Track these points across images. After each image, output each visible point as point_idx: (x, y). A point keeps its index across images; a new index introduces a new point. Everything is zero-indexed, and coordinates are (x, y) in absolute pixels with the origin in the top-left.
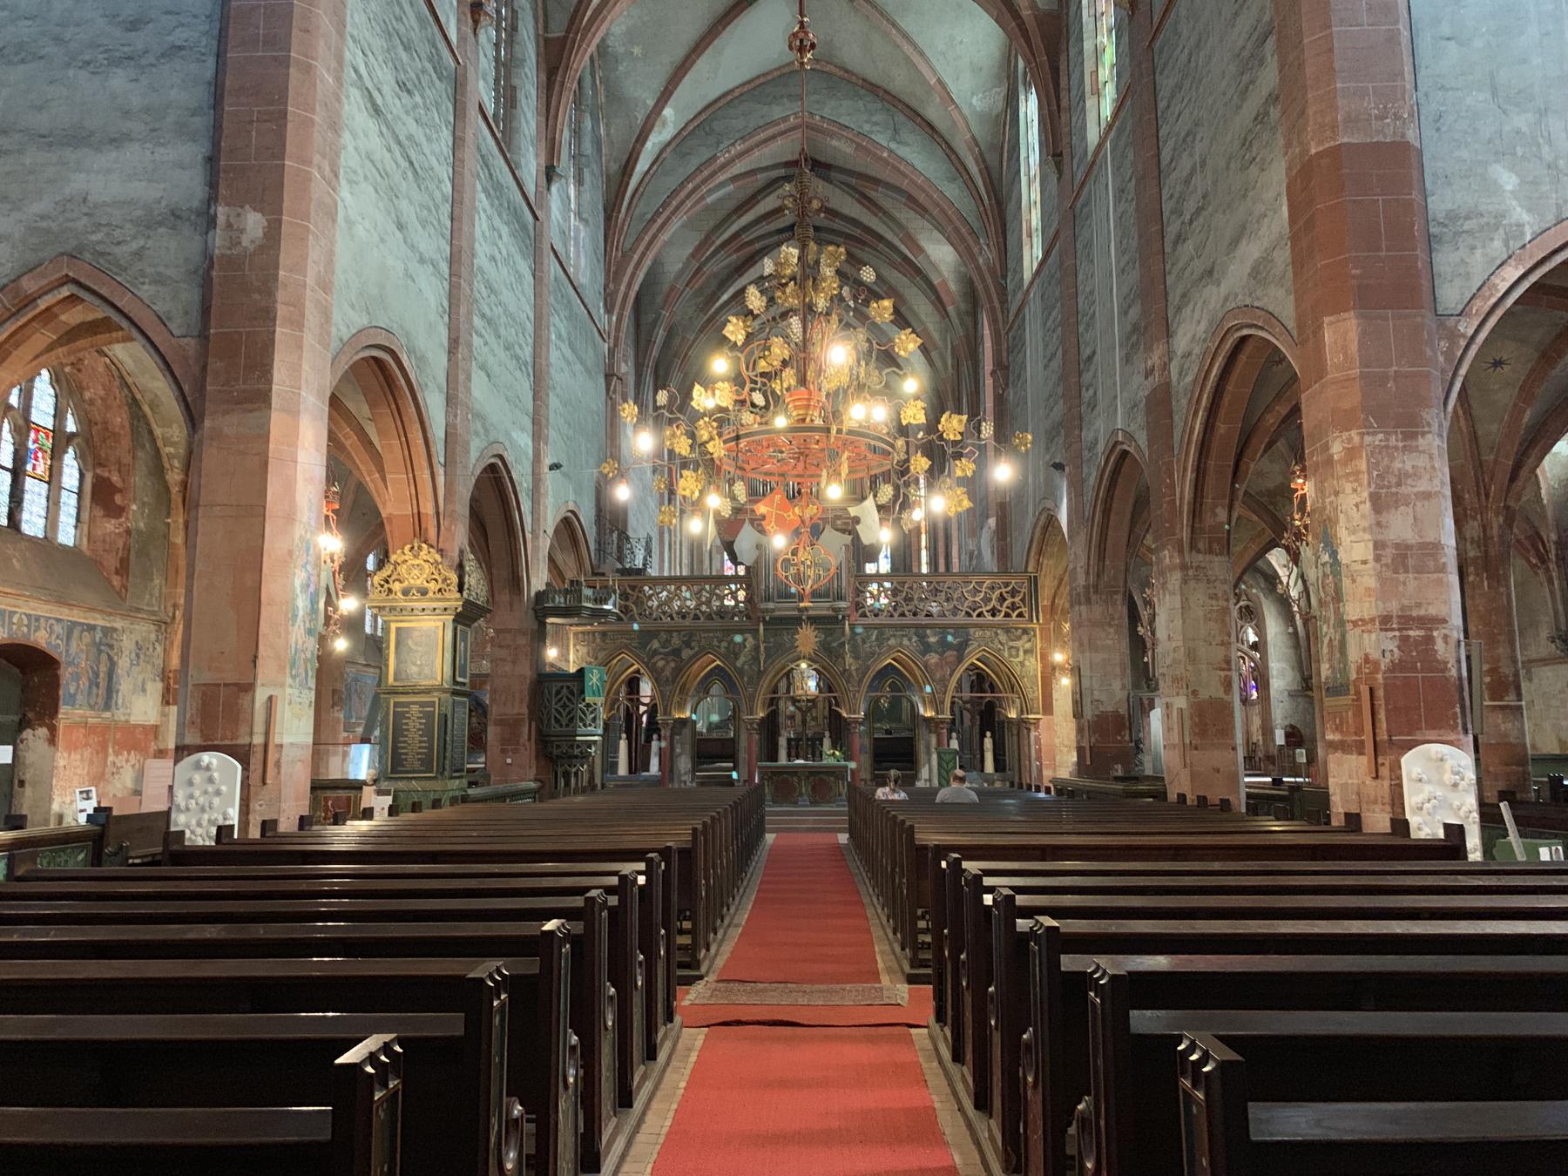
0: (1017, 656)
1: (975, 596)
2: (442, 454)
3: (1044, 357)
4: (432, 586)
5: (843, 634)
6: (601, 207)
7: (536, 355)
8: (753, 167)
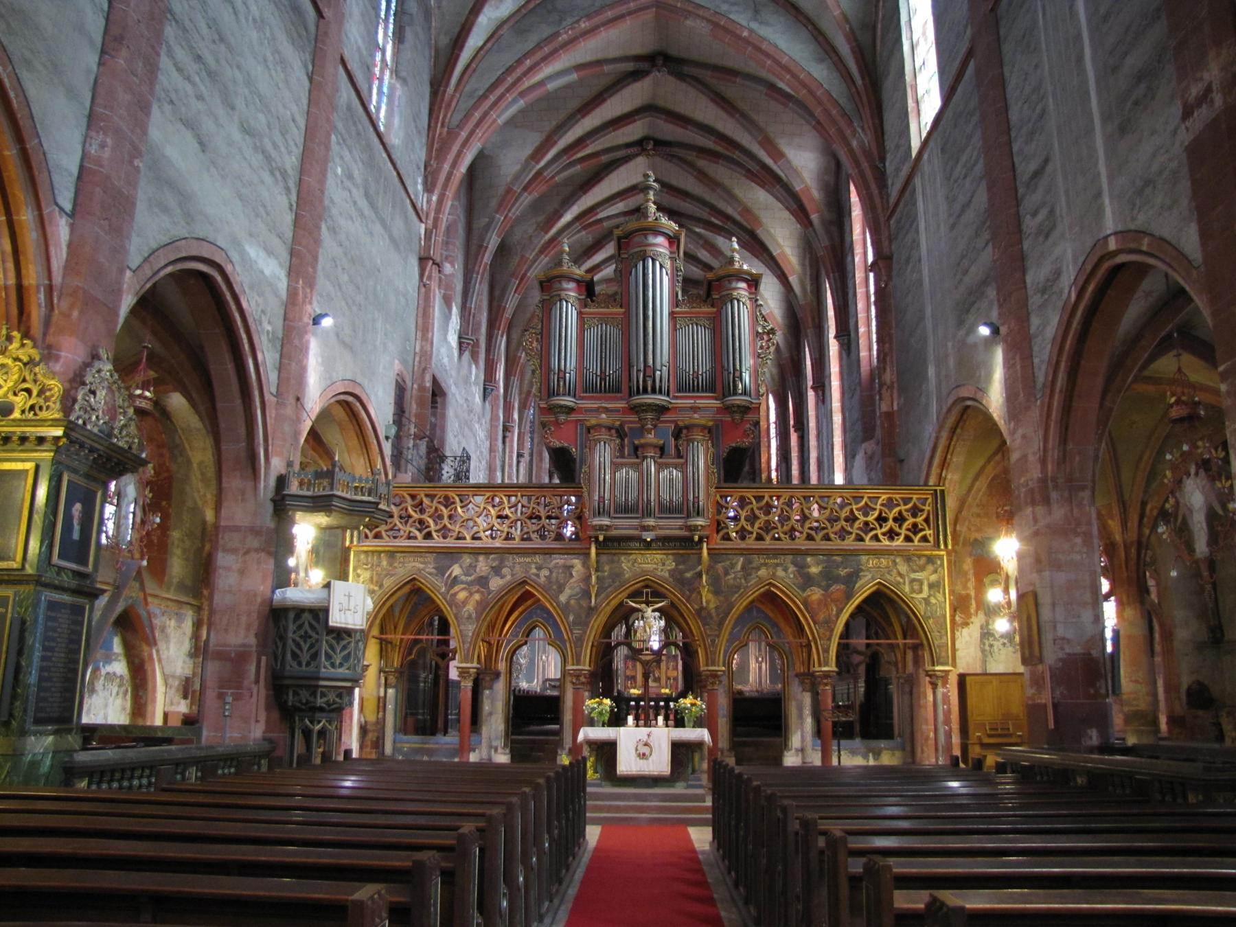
0: (921, 591)
1: (866, 515)
2: (70, 194)
3: (950, 215)
4: (20, 401)
5: (699, 562)
6: (426, 78)
7: (303, 170)
8: (600, 56)
